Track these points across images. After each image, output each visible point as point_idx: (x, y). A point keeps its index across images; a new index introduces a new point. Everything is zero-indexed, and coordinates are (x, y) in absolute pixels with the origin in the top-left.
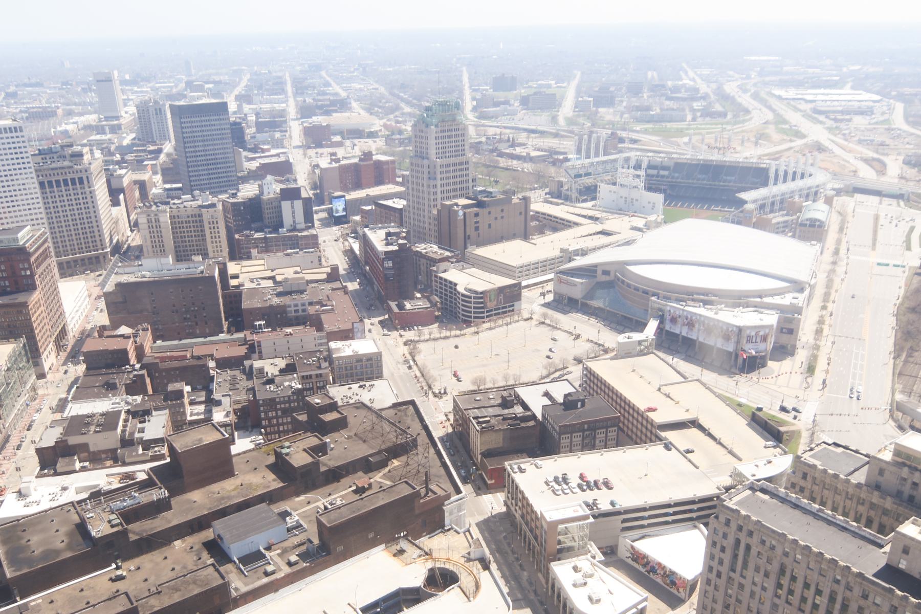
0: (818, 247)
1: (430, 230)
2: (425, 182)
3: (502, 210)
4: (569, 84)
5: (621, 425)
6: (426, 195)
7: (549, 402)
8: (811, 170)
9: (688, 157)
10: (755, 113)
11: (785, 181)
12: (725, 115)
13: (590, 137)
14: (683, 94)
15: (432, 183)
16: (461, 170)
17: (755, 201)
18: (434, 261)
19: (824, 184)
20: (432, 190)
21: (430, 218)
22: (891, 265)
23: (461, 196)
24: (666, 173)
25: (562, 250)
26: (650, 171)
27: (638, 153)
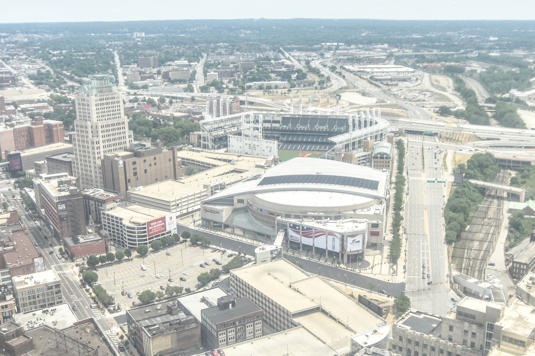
1: (96, 177)
3: (155, 159)
4: (198, 62)
8: (375, 119)
10: (333, 81)
13: (218, 101)
14: (284, 69)
15: (95, 139)
17: (341, 143)
19: (386, 129)
20: (96, 146)
21: (95, 167)
24: (277, 125)
25: (205, 186)
27: (256, 112)
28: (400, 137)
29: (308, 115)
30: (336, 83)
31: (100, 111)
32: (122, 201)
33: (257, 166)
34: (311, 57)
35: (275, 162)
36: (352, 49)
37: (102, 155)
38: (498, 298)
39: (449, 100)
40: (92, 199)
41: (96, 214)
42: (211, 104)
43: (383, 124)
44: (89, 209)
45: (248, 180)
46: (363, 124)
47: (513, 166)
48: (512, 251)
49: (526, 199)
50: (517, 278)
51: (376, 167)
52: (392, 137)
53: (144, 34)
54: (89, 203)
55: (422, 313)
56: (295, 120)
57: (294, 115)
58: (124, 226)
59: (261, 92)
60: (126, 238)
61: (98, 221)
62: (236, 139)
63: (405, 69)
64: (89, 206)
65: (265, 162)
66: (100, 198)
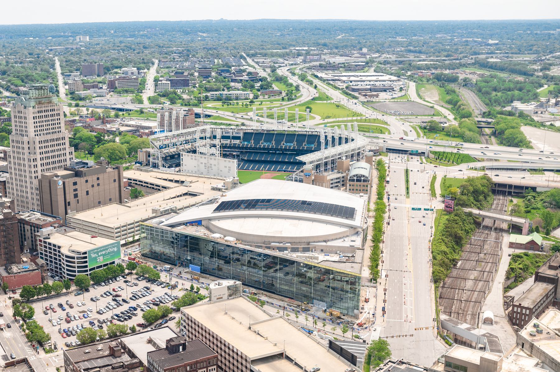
0: (366, 197)
1: (33, 199)
2: (25, 157)
3: (98, 179)
4: (148, 69)
5: (219, 364)
6: (27, 168)
7: (153, 349)
8: (353, 135)
9: (254, 128)
11: (333, 145)
12: (281, 93)
13: (170, 113)
14: (245, 77)
16: (58, 145)
17: (311, 162)
18: (38, 227)
19: (364, 147)
20: (33, 164)
21: (32, 188)
22: (422, 209)
23: (60, 167)
25: (154, 211)
26: (225, 142)
27: (212, 126)
28: (380, 157)
29: (273, 130)
30: (307, 93)
31: (38, 124)
32: (61, 226)
33: (214, 189)
34: (277, 63)
35: (235, 185)
36: (326, 54)
37: (39, 174)
38: (494, 348)
39: (438, 114)
40: (28, 223)
41: (32, 241)
42: (163, 116)
43: (361, 141)
44: (25, 235)
45: (203, 204)
46: (337, 141)
47: (514, 192)
48: (511, 293)
49: (531, 231)
50: (517, 325)
51: (353, 191)
52: (371, 157)
53: (88, 37)
54: (24, 228)
55: (403, 363)
56: (258, 135)
57: (257, 130)
58: (63, 255)
59: (219, 104)
60: (64, 268)
61: (33, 249)
62: (190, 156)
63: (387, 77)
64: (24, 231)
65: (222, 184)
66: (37, 222)
